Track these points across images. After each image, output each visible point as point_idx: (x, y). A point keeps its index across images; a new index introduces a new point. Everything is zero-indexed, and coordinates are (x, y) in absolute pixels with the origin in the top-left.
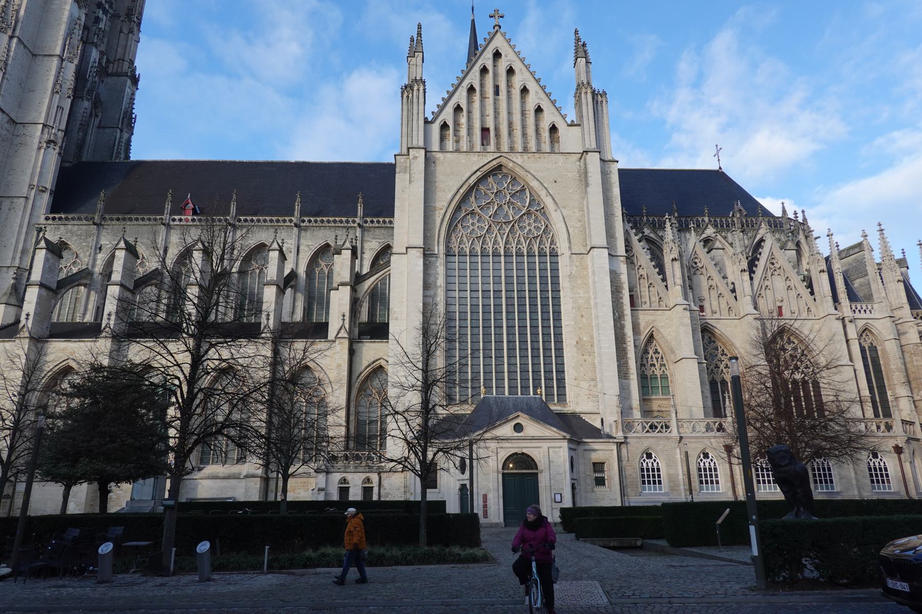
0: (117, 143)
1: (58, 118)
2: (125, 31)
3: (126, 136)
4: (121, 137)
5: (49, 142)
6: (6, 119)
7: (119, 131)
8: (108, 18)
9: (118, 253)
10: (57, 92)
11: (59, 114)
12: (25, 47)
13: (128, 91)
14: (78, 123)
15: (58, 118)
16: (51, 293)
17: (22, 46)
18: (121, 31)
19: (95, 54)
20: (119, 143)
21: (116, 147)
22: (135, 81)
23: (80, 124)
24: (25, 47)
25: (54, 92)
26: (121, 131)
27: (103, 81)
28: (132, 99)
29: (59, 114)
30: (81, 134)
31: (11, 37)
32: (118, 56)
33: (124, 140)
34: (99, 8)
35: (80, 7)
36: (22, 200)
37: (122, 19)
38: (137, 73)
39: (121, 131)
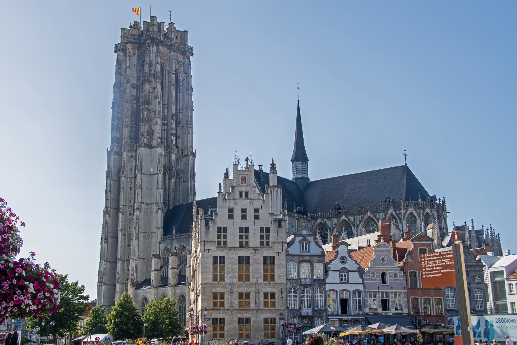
0: (190, 188)
1: (160, 198)
2: (186, 133)
3: (193, 183)
4: (191, 185)
5: (158, 209)
6: (145, 204)
7: (190, 182)
8: (180, 129)
9: (170, 258)
10: (158, 189)
11: (160, 197)
12: (146, 174)
13: (191, 161)
14: (172, 189)
15: (160, 198)
16: (159, 271)
17: (145, 175)
18: (185, 134)
19: (173, 157)
20: (191, 187)
21: (190, 190)
22: (194, 155)
23: (173, 190)
24: (146, 174)
25: (157, 188)
26: (191, 181)
27: (182, 161)
28: (194, 162)
29: (160, 197)
30: (173, 194)
31: (141, 174)
32: (186, 147)
33: (192, 186)
34: (172, 136)
35: (161, 148)
36: (154, 233)
37: (185, 127)
38: (194, 151)
39: (191, 181)
